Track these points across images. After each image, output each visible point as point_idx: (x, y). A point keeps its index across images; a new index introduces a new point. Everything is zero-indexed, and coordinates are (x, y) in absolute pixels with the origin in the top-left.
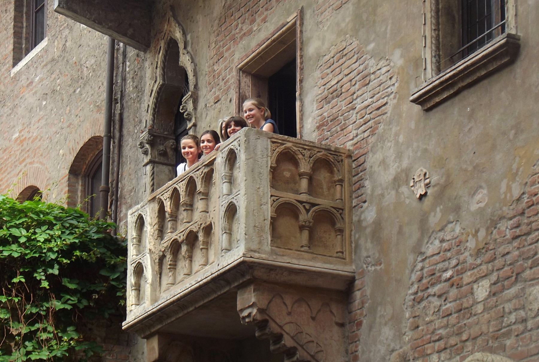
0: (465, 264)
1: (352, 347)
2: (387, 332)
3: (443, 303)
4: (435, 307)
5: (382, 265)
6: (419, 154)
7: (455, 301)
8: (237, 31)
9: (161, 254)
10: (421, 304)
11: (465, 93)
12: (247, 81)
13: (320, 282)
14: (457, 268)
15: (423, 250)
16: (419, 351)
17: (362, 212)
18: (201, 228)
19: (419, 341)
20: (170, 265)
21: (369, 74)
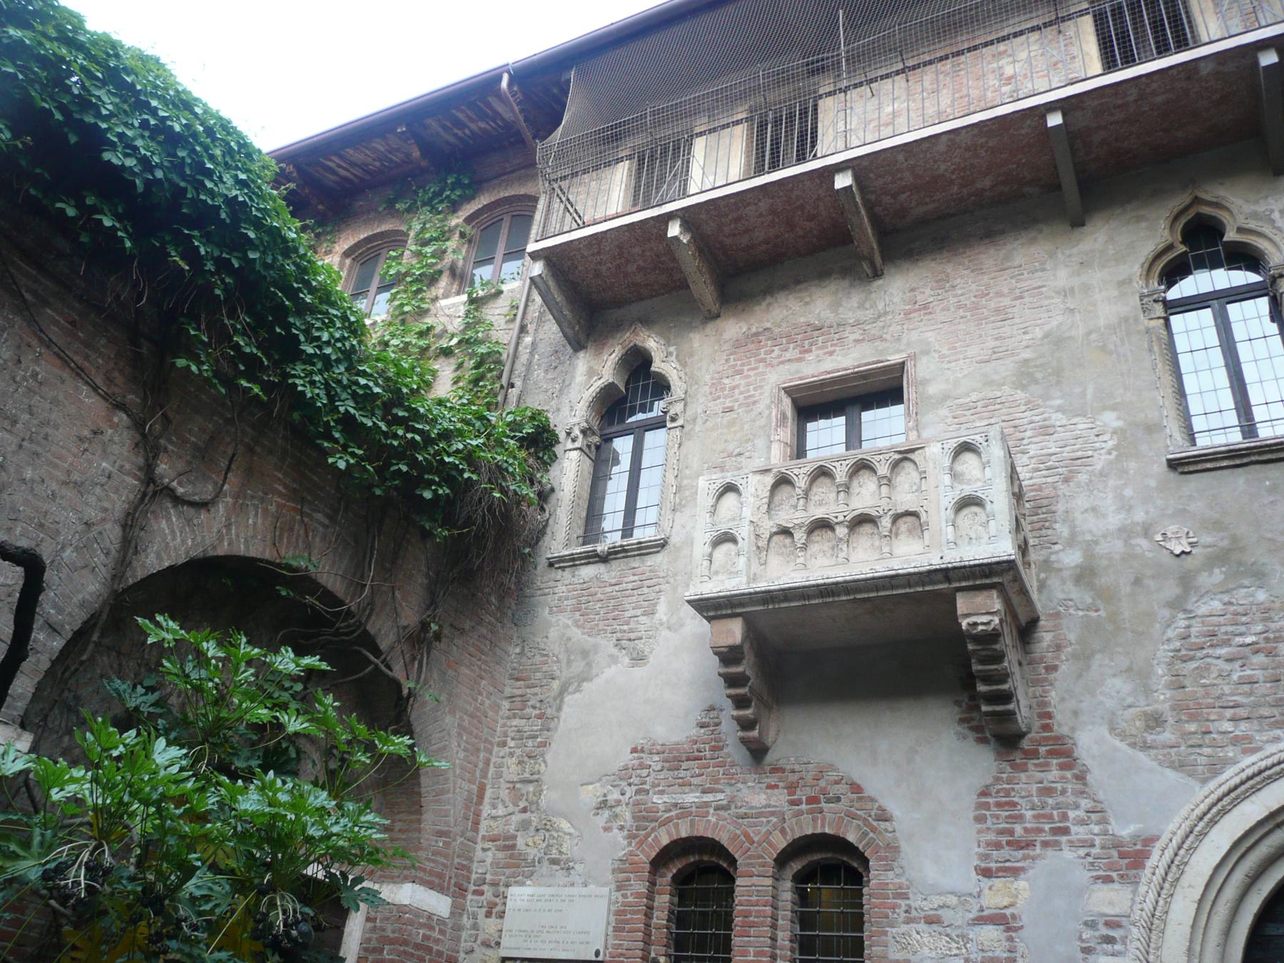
1: (1039, 690)
3: (1239, 669)
6: (1170, 512)
8: (773, 355)
9: (775, 530)
10: (1189, 663)
11: (1258, 467)
12: (787, 403)
15: (1189, 607)
17: (1052, 553)
18: (890, 513)
21: (1054, 426)
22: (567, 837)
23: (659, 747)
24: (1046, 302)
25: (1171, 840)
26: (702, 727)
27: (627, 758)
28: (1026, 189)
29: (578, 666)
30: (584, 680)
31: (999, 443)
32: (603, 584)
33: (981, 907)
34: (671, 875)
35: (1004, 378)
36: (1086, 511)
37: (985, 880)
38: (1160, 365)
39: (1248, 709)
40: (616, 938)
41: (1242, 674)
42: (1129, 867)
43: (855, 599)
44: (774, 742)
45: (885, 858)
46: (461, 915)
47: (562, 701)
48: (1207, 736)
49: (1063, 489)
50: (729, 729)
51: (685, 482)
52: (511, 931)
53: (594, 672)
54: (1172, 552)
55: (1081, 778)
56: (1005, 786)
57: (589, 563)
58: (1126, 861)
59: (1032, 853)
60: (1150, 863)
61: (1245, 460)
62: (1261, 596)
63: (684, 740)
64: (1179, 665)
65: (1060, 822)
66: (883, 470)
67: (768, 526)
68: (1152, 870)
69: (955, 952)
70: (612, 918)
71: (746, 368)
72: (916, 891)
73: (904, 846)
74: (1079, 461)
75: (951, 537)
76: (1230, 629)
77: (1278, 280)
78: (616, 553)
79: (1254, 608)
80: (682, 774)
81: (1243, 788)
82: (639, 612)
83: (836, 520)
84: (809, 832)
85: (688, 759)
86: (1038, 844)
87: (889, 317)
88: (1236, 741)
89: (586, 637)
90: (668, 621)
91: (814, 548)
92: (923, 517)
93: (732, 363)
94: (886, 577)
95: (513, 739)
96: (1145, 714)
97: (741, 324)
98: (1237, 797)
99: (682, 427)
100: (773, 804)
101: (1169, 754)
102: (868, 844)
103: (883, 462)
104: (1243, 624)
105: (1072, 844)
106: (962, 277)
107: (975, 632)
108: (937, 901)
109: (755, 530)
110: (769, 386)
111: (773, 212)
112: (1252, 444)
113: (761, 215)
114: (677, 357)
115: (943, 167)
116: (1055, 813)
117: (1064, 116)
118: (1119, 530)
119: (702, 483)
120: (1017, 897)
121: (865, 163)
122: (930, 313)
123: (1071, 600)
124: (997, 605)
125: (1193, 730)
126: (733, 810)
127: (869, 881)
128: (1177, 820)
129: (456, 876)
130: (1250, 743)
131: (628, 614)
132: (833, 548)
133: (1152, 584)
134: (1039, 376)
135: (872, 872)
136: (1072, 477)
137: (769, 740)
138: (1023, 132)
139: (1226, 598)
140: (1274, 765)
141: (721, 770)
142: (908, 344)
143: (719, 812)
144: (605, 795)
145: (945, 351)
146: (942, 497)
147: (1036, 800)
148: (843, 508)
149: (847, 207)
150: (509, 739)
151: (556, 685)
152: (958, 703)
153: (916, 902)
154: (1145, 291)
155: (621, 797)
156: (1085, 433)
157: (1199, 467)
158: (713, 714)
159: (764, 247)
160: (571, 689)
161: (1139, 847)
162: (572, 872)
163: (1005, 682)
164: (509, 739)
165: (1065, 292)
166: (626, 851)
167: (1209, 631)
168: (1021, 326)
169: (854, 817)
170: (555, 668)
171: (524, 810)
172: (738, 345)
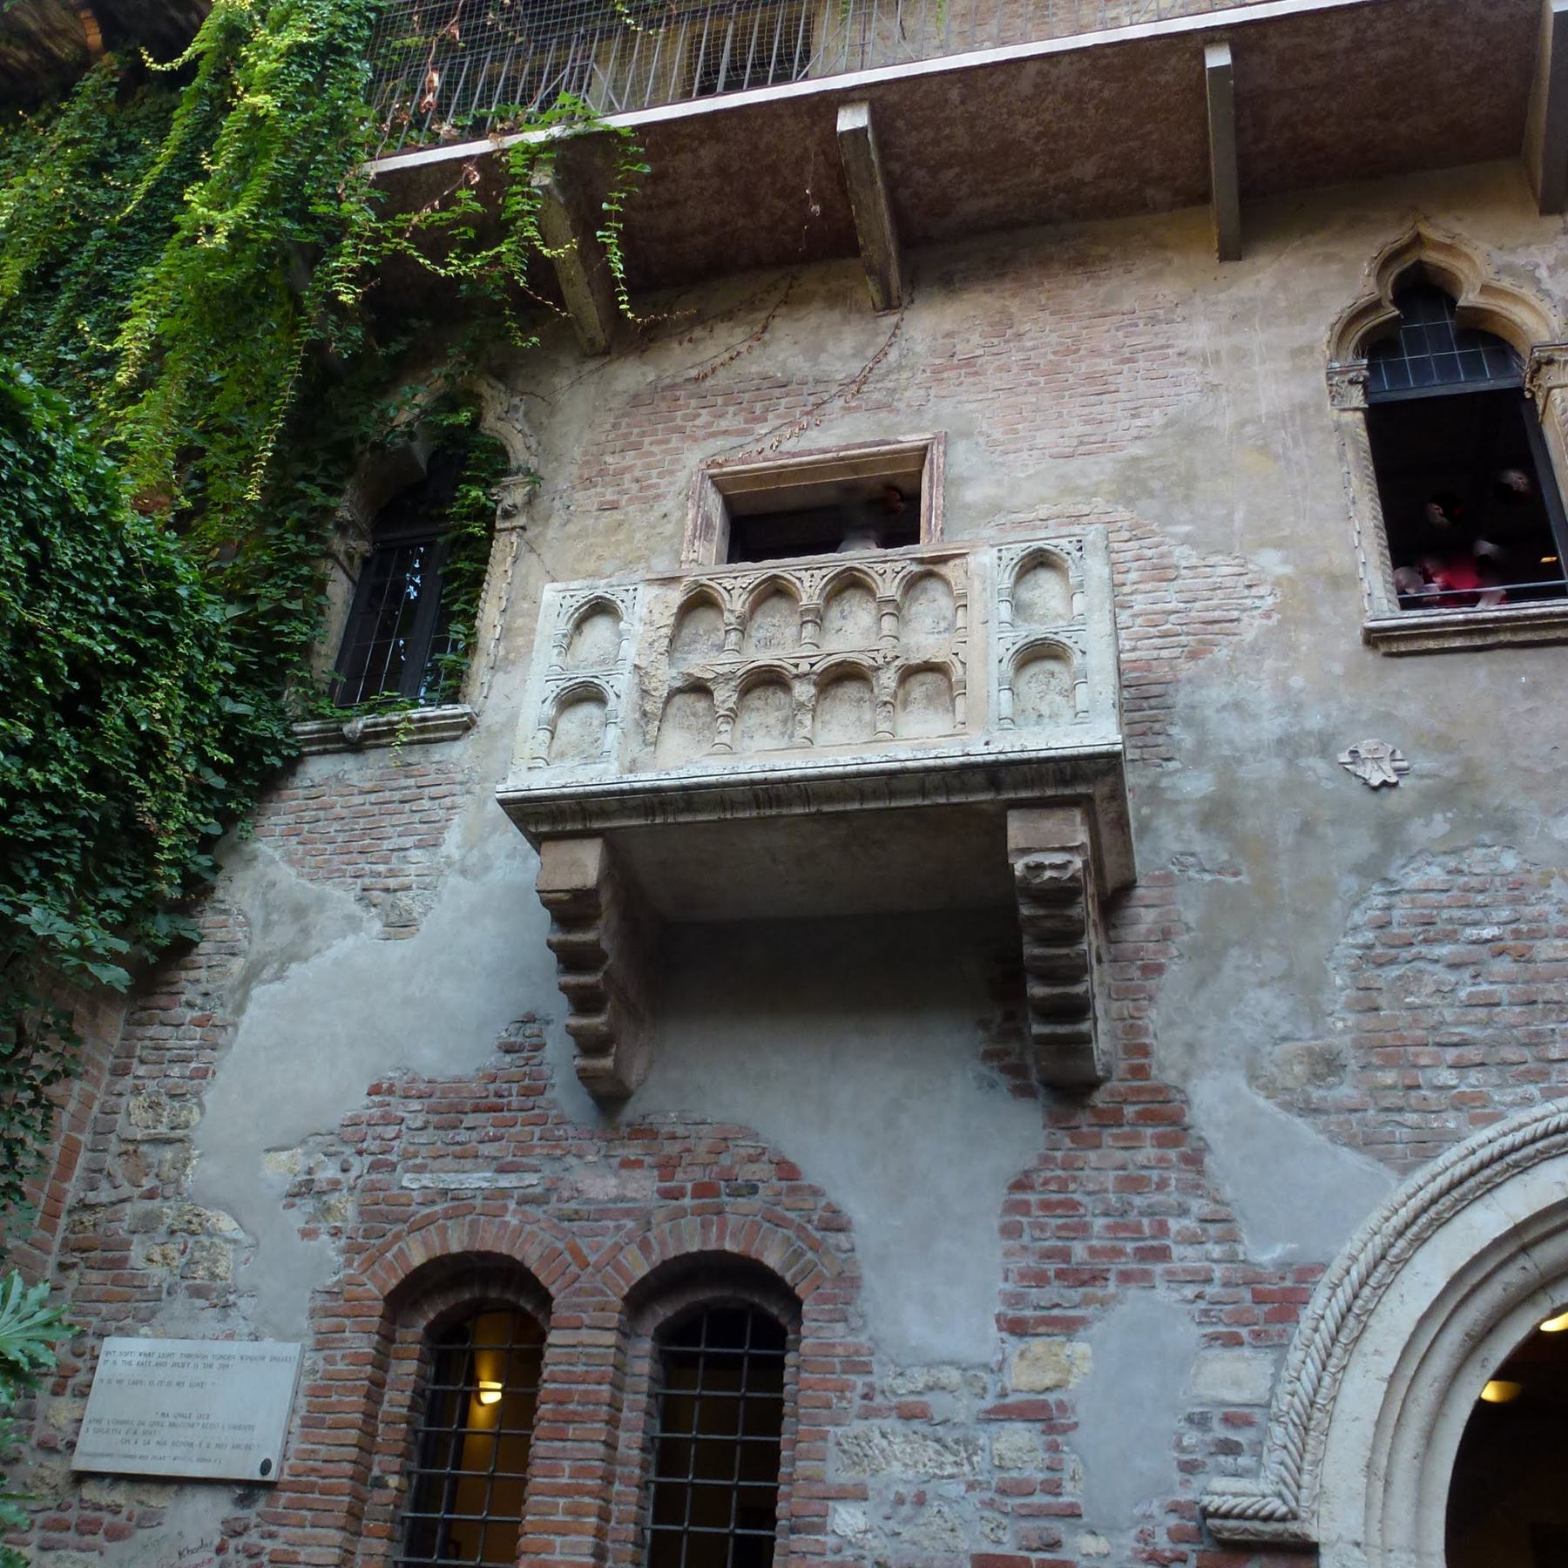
0: (1543, 925)
1: (1128, 1007)
3: (1469, 981)
4: (1443, 983)
5: (1240, 878)
6: (1364, 717)
7: (1512, 983)
8: (697, 422)
9: (678, 684)
13: (1109, 861)
14: (1514, 926)
15: (1392, 875)
16: (1388, 1055)
17: (1162, 775)
19: (1388, 1036)
20: (731, 710)
21: (1177, 567)
22: (230, 1247)
23: (422, 1086)
24: (1172, 372)
25: (1348, 1272)
26: (507, 1052)
27: (359, 1103)
28: (1150, 192)
29: (283, 934)
30: (290, 956)
31: (1102, 553)
32: (348, 790)
33: (1004, 1388)
34: (423, 1323)
35: (1097, 484)
36: (1224, 707)
37: (1013, 1340)
38: (1355, 482)
39: (1483, 1049)
40: (305, 1438)
41: (1473, 989)
42: (1271, 1318)
43: (819, 813)
44: (641, 1083)
45: (833, 1299)
47: (246, 996)
48: (1413, 1093)
49: (1187, 668)
50: (559, 1056)
51: (519, 622)
52: (99, 1421)
53: (314, 943)
54: (1366, 783)
55: (1194, 1160)
56: (1060, 1172)
57: (325, 752)
58: (1266, 1308)
59: (1100, 1292)
60: (1307, 1314)
61: (1490, 640)
62: (1509, 861)
63: (472, 1073)
64: (1370, 973)
65: (1153, 1237)
66: (889, 588)
67: (666, 676)
68: (1312, 1324)
69: (949, 1470)
70: (302, 1401)
71: (647, 440)
72: (885, 1359)
73: (869, 1276)
74: (1217, 627)
75: (1006, 710)
76: (1457, 913)
77: (1544, 369)
78: (378, 735)
79: (1497, 880)
80: (463, 1136)
81: (1472, 1182)
82: (408, 841)
83: (795, 671)
84: (694, 1247)
85: (474, 1111)
86: (1112, 1276)
87: (906, 375)
88: (1461, 1103)
89: (303, 881)
90: (463, 859)
91: (750, 720)
92: (957, 673)
93: (623, 430)
94: (882, 773)
95: (142, 1062)
96: (1310, 1051)
97: (645, 369)
98: (1463, 1198)
99: (523, 528)
100: (630, 1194)
101: (1348, 1122)
102: (803, 1270)
103: (890, 575)
104: (1478, 906)
105: (1172, 1279)
106: (1035, 321)
107: (1038, 880)
108: (920, 1379)
109: (641, 683)
110: (687, 471)
111: (721, 170)
112: (1504, 614)
113: (700, 174)
114: (525, 415)
115: (1022, 126)
116: (1145, 1221)
117: (1234, 57)
118: (1280, 741)
119: (550, 594)
120: (1069, 1371)
121: (893, 98)
122: (976, 373)
123: (1192, 855)
124: (1082, 837)
125: (1389, 1081)
126: (553, 1204)
127: (798, 1341)
128: (1359, 1236)
130: (1484, 1106)
131: (386, 845)
132: (785, 722)
133: (1330, 833)
134: (1156, 484)
135: (806, 1323)
136: (1205, 652)
137: (633, 1078)
138: (1162, 79)
139: (1452, 863)
140: (1524, 1144)
141: (537, 1131)
142: (936, 420)
143: (526, 1208)
144: (310, 1171)
145: (997, 435)
146: (993, 640)
147: (1112, 1198)
148: (808, 650)
149: (853, 168)
150: (135, 1061)
151: (237, 965)
152: (983, 1024)
154: (1336, 365)
155: (340, 1176)
156: (1229, 582)
157: (1415, 646)
158: (531, 1029)
160: (265, 975)
161: (1288, 1283)
162: (233, 1312)
163: (1076, 979)
164: (135, 1061)
165: (1205, 359)
166: (341, 1275)
167: (1423, 915)
168: (1130, 405)
169: (780, 1223)
170: (240, 935)
171: (151, 1195)
172: (636, 401)
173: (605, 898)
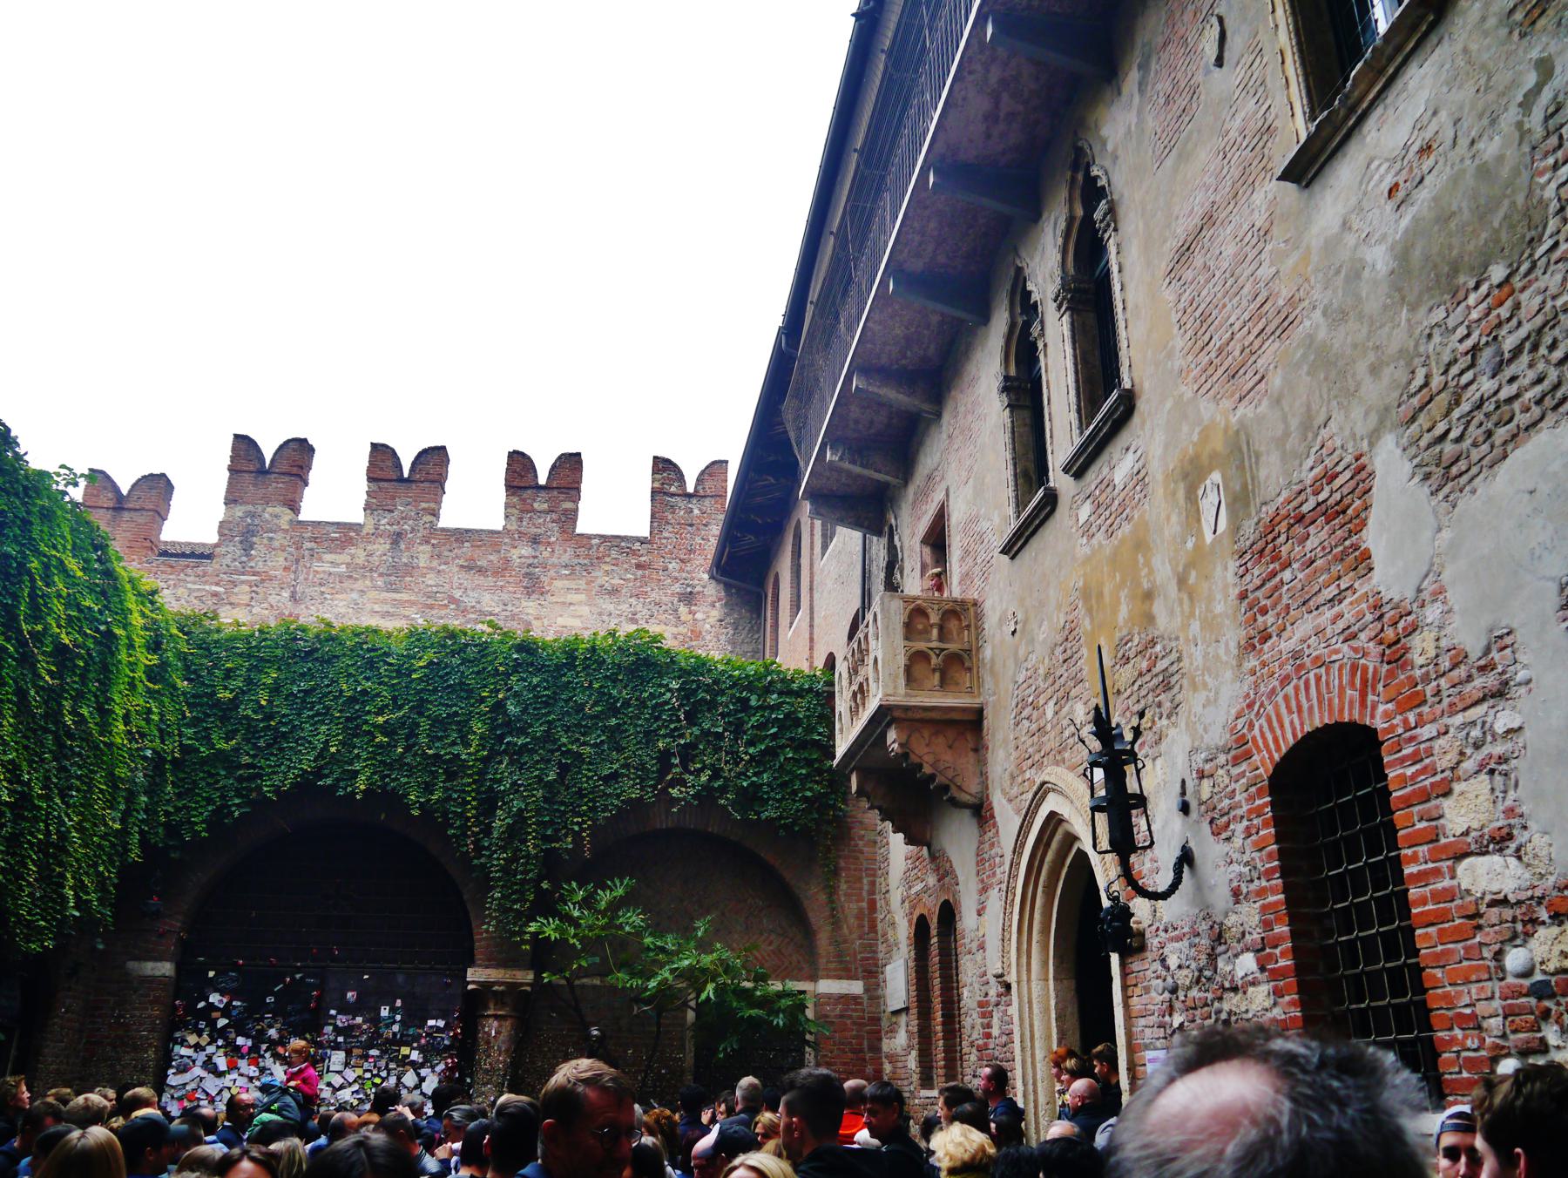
2: (1001, 754)
12: (927, 550)
46: (876, 989)
129: (862, 966)
153: (967, 941)
159: (895, 421)
173: (868, 788)
